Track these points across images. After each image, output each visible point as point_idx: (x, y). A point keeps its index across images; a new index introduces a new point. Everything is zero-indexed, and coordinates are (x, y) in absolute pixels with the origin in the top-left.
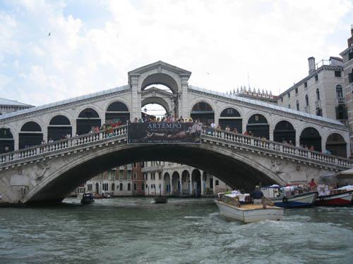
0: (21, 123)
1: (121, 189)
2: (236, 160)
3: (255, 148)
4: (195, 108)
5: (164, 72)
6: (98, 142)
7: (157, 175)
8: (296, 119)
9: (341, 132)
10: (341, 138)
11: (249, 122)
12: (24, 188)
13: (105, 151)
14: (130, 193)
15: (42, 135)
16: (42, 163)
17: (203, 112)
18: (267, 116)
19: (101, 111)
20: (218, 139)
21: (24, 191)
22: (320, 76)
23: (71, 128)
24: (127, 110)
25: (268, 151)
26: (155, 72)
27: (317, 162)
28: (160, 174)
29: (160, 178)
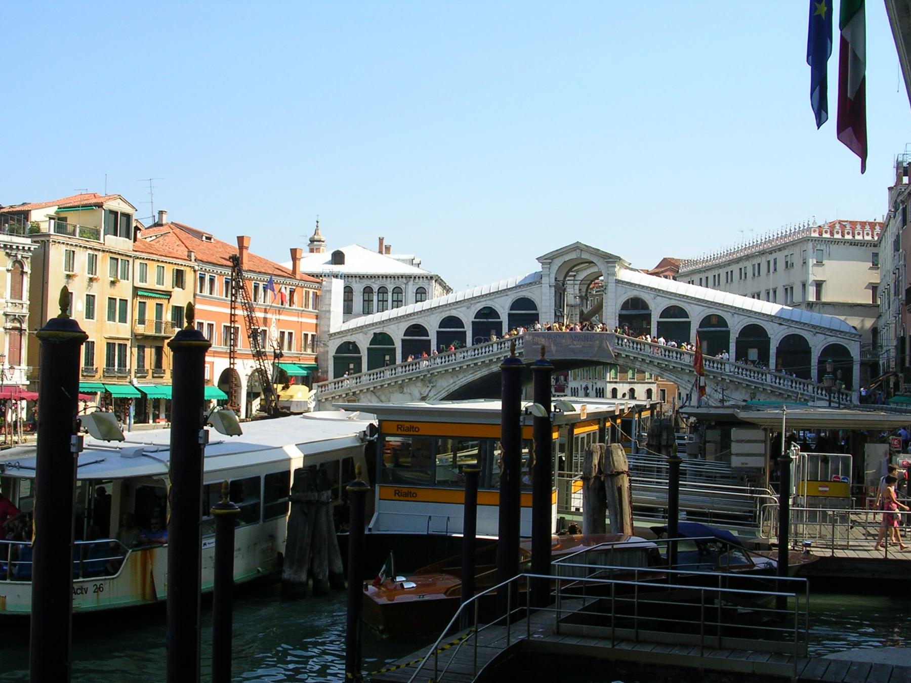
0: (404, 326)
4: (625, 306)
5: (585, 256)
9: (847, 341)
11: (701, 325)
15: (429, 341)
18: (727, 317)
19: (502, 311)
20: (639, 354)
24: (536, 310)
27: (780, 389)
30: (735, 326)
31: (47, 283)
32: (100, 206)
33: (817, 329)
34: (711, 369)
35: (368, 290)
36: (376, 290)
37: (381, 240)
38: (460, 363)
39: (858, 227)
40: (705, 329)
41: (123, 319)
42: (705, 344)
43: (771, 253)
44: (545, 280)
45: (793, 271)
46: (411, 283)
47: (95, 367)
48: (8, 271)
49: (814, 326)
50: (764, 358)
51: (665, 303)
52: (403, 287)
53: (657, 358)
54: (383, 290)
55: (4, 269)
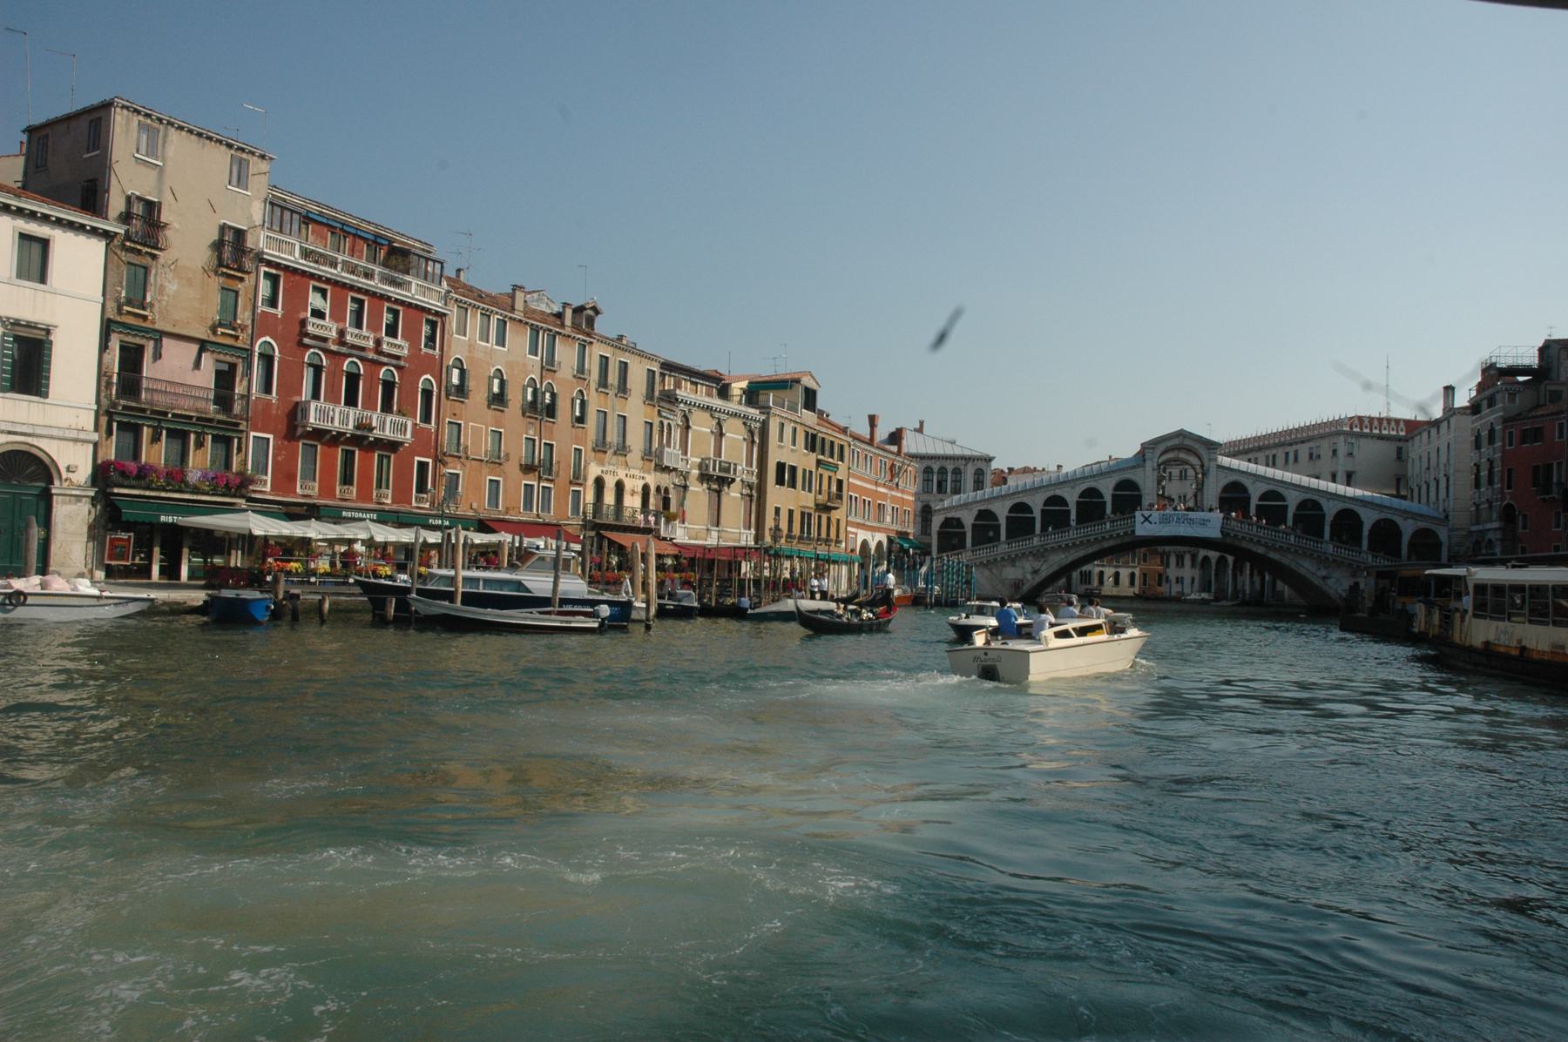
0: (1009, 504)
1: (1117, 582)
2: (1271, 560)
4: (1226, 489)
5: (1188, 442)
7: (1187, 558)
10: (1434, 534)
13: (1112, 543)
16: (1040, 554)
17: (1234, 497)
18: (1323, 502)
22: (1453, 420)
23: (1068, 512)
26: (1176, 442)
28: (1194, 557)
29: (1193, 565)
30: (1331, 510)
32: (798, 381)
33: (1406, 514)
44: (1149, 464)
49: (1405, 512)
54: (943, 471)
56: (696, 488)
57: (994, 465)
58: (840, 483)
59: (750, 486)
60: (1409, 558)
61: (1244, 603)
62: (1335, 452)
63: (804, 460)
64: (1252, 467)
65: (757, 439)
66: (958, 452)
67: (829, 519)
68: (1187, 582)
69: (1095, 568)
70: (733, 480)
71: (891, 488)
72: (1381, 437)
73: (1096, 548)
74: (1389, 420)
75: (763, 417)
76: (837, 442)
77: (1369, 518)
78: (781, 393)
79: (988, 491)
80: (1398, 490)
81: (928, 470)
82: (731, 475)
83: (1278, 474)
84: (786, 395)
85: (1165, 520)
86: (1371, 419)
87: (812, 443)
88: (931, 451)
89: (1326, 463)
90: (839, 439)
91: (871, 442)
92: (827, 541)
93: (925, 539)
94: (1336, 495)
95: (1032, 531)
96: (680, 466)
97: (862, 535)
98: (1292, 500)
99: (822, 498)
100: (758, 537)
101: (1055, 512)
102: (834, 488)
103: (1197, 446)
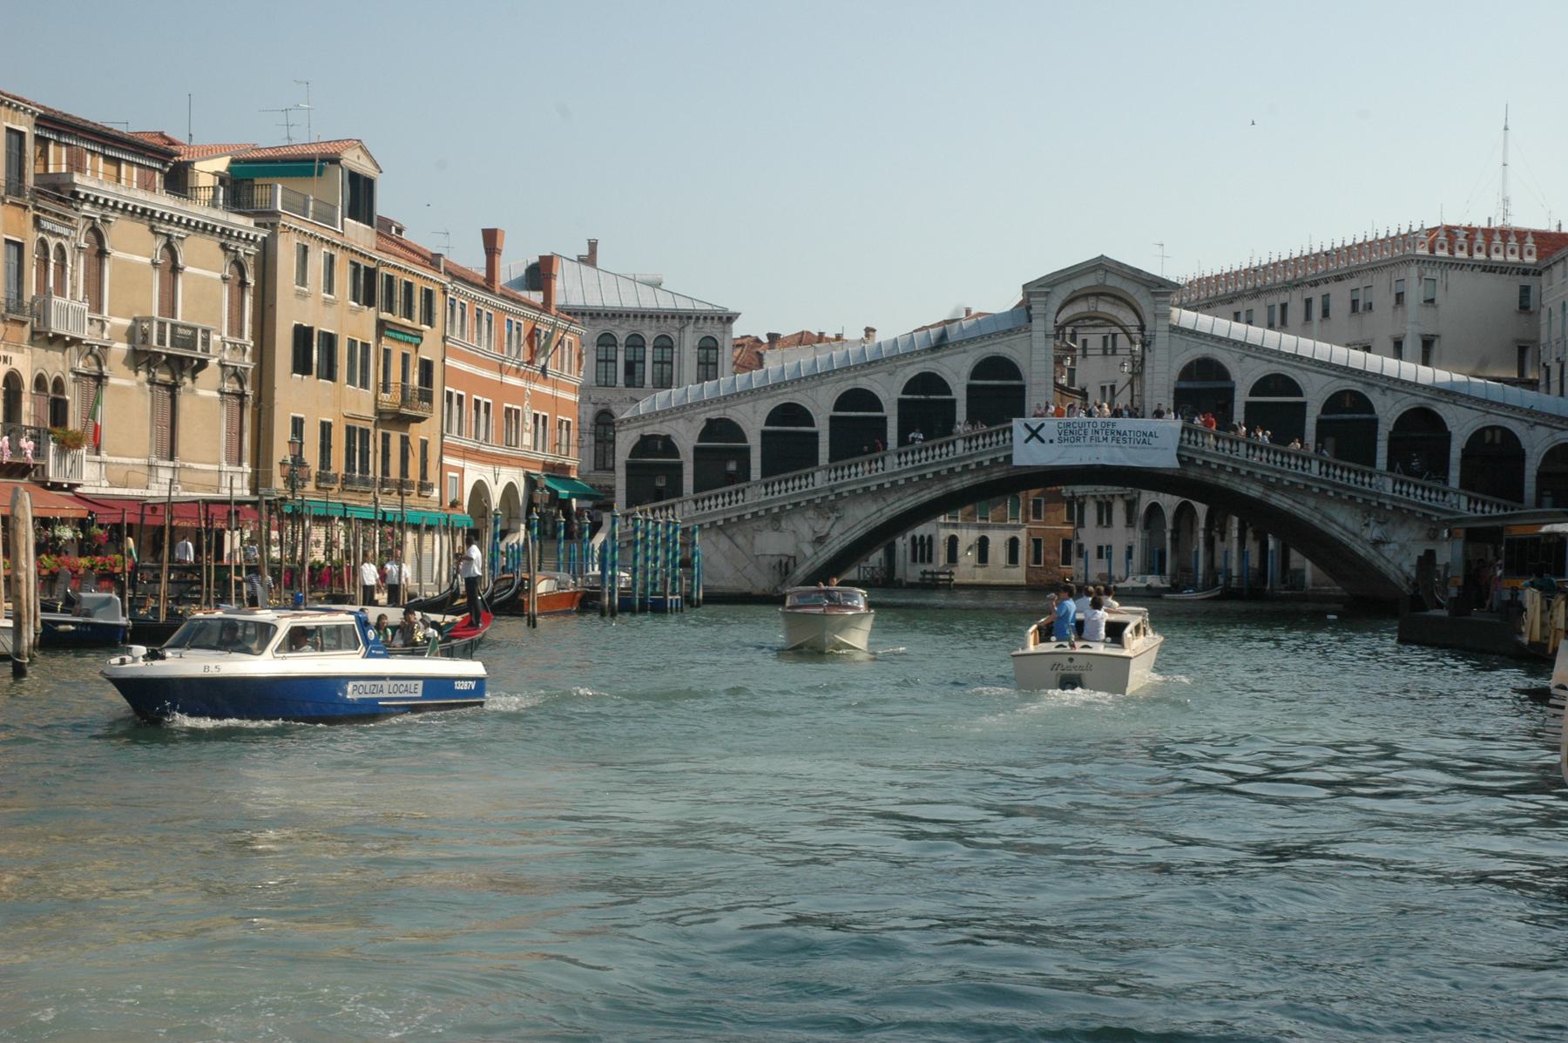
0: (766, 406)
1: (983, 557)
3: (1323, 481)
4: (1187, 372)
5: (1112, 281)
6: (951, 461)
8: (1455, 403)
12: (784, 560)
14: (1018, 575)
15: (816, 435)
16: (828, 505)
17: (1203, 390)
18: (1374, 397)
21: (784, 568)
23: (884, 420)
25: (1351, 489)
26: (1089, 281)
28: (1131, 506)
29: (1130, 522)
30: (1388, 411)
31: (273, 306)
34: (1359, 486)
35: (606, 341)
36: (622, 340)
37: (593, 246)
38: (894, 474)
39: (1497, 239)
40: (1333, 417)
41: (364, 384)
42: (1330, 441)
43: (1316, 284)
44: (1037, 324)
45: (1368, 318)
46: (690, 329)
47: (332, 472)
48: (224, 279)
49: (1530, 412)
50: (1439, 468)
51: (1262, 369)
52: (674, 335)
53: (1261, 467)
54: (636, 342)
55: (218, 276)
56: (123, 380)
57: (738, 330)
58: (426, 367)
59: (239, 376)
60: (1539, 504)
61: (1229, 594)
62: (1400, 297)
63: (352, 323)
64: (1239, 330)
65: (250, 280)
66: (665, 303)
67: (405, 441)
68: (1119, 554)
69: (938, 530)
70: (203, 364)
71: (530, 378)
72: (1489, 268)
73: (936, 491)
74: (1505, 233)
75: (262, 234)
76: (418, 285)
77: (1461, 425)
78: (300, 185)
79: (727, 380)
80: (1521, 371)
81: (606, 341)
82: (199, 353)
83: (1288, 342)
84: (311, 189)
85: (1070, 435)
86: (1471, 232)
87: (367, 286)
88: (612, 302)
89: (1383, 322)
90: (423, 278)
91: (488, 284)
92: (402, 486)
93: (602, 478)
94: (1397, 380)
95: (813, 460)
96: (88, 334)
97: (474, 473)
98: (1315, 392)
99: (390, 399)
100: (258, 481)
101: (857, 426)
102: (414, 380)
103: (1130, 289)
